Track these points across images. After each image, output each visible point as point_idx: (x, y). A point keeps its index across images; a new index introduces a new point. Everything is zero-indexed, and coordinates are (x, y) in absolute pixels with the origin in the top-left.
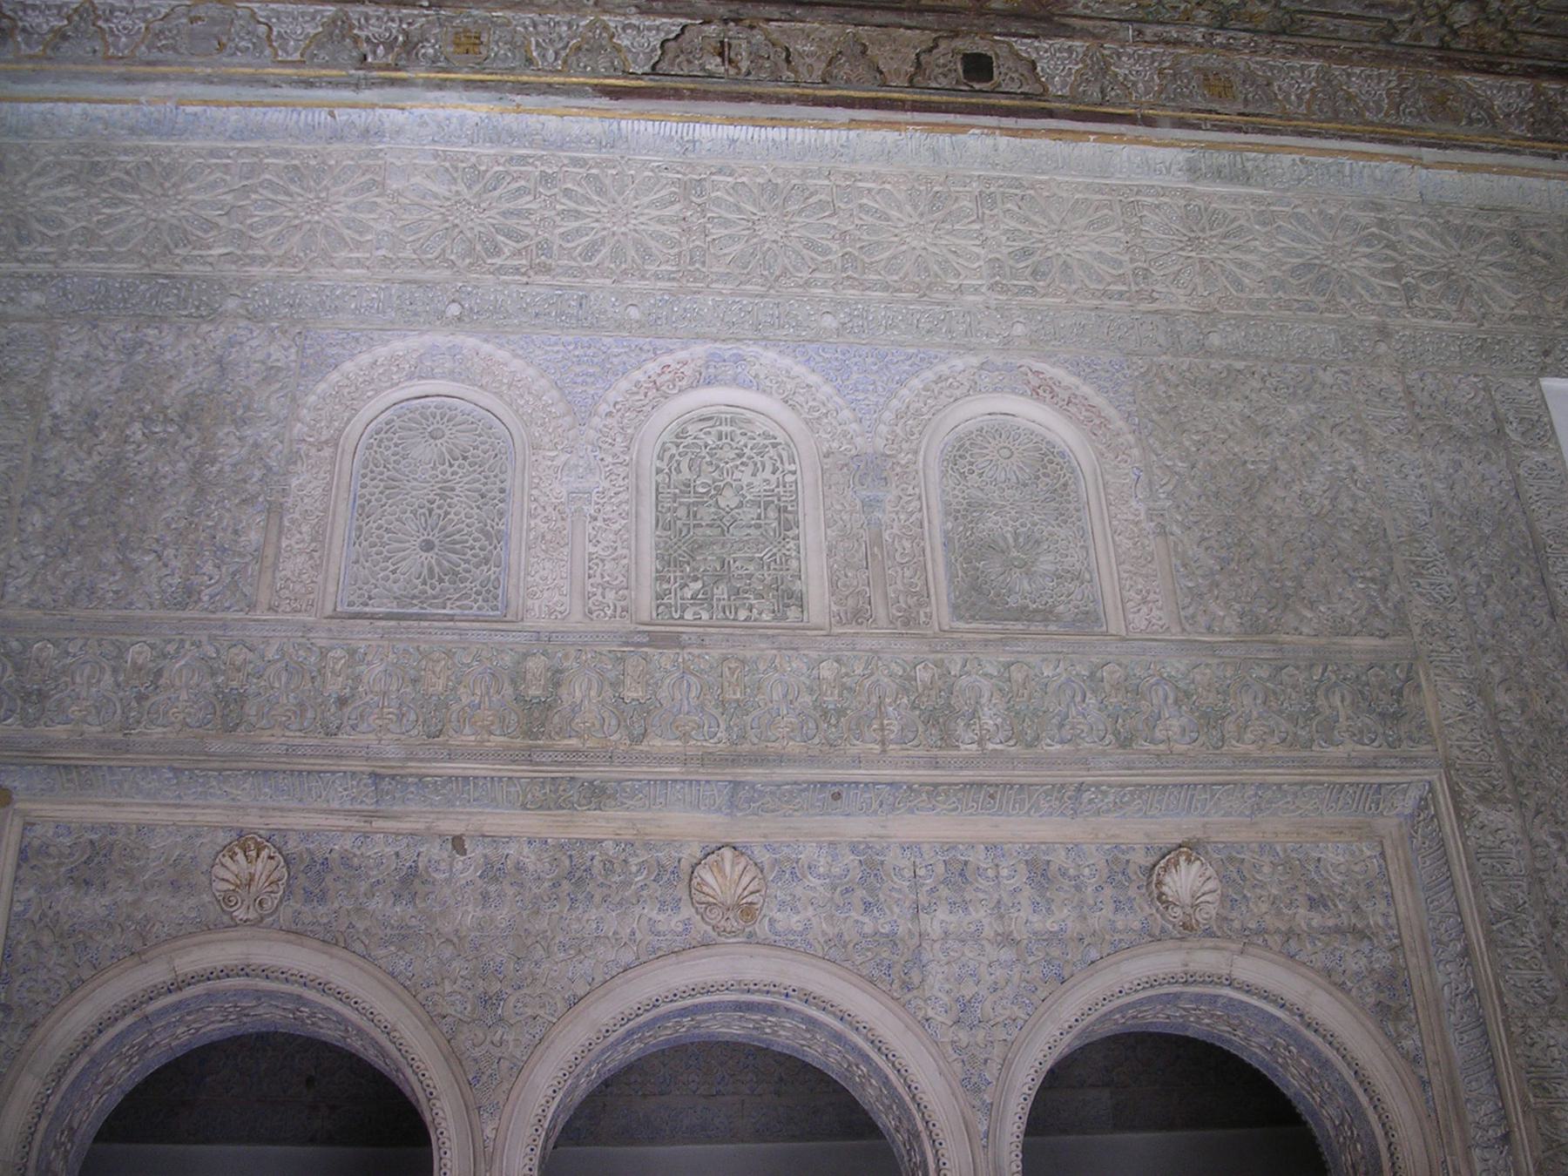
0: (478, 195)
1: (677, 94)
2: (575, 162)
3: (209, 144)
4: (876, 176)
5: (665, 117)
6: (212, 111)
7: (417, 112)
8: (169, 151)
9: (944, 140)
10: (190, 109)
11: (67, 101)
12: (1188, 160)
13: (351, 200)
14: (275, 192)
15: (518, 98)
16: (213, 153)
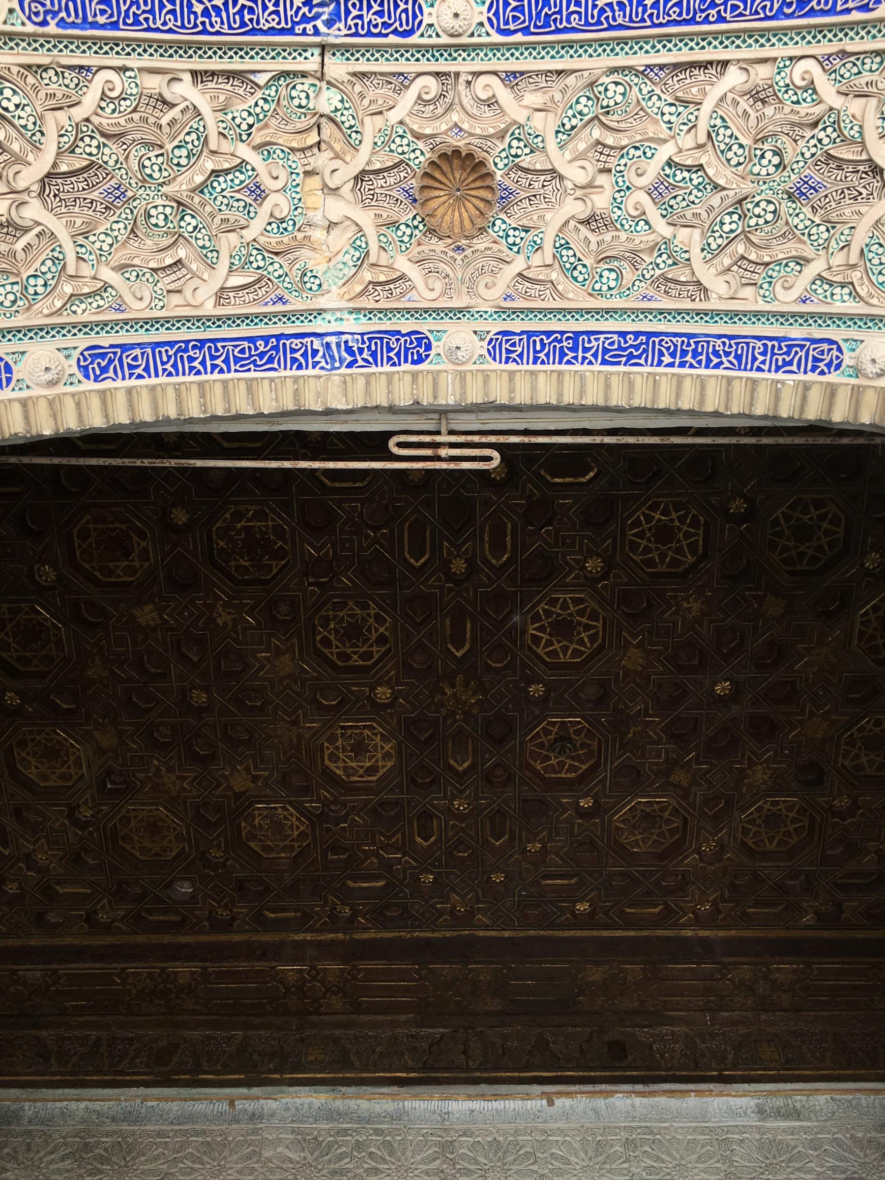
0: (316, 1159)
1: (438, 1082)
2: (377, 1132)
3: (157, 1128)
4: (561, 1132)
5: (431, 1098)
6: (163, 1105)
7: (284, 1101)
8: (134, 1133)
9: (600, 1103)
10: (150, 1104)
11: (77, 1100)
12: (757, 1105)
13: (240, 1166)
14: (194, 1162)
15: (344, 1089)
16: (159, 1135)
